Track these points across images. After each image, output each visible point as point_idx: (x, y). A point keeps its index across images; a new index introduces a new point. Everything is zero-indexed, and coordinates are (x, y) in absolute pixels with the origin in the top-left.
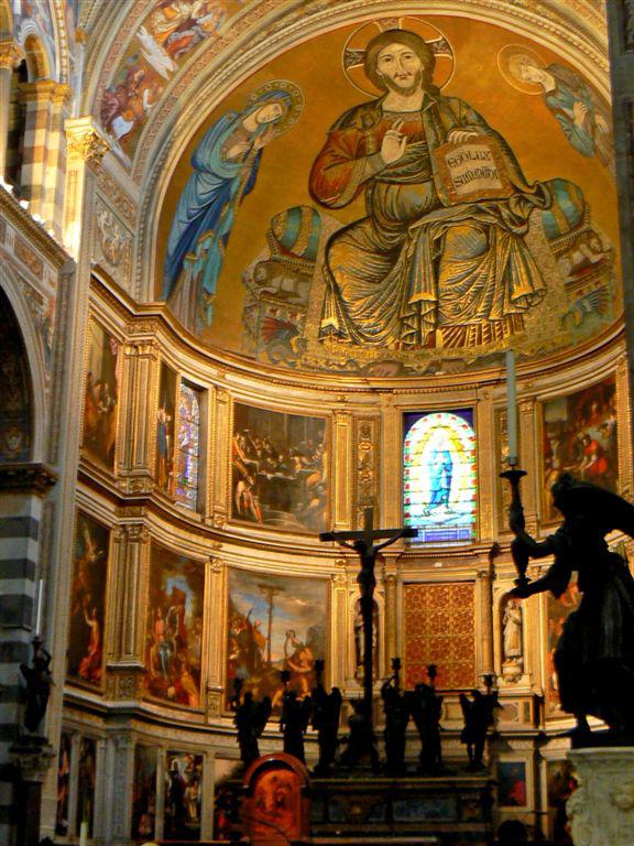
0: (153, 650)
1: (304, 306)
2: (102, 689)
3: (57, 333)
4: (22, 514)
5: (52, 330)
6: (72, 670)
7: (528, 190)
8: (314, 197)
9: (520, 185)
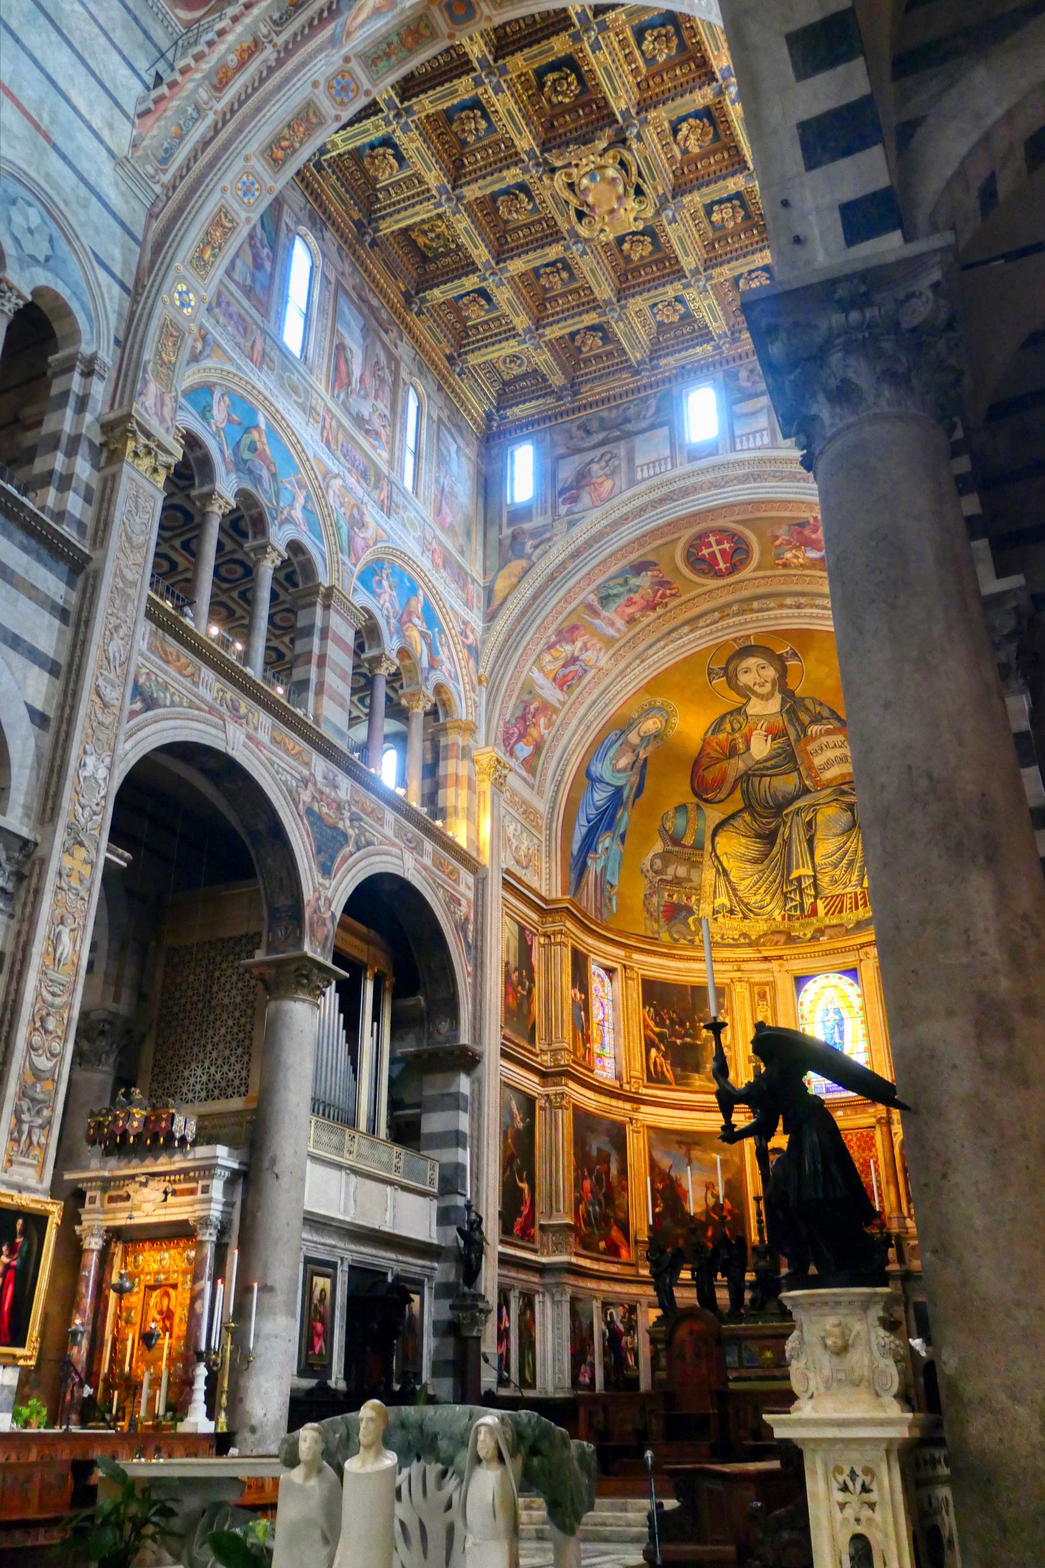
0: (581, 1207)
2: (537, 1246)
3: (476, 929)
4: (453, 1090)
5: (471, 927)
6: (506, 1229)
8: (696, 794)
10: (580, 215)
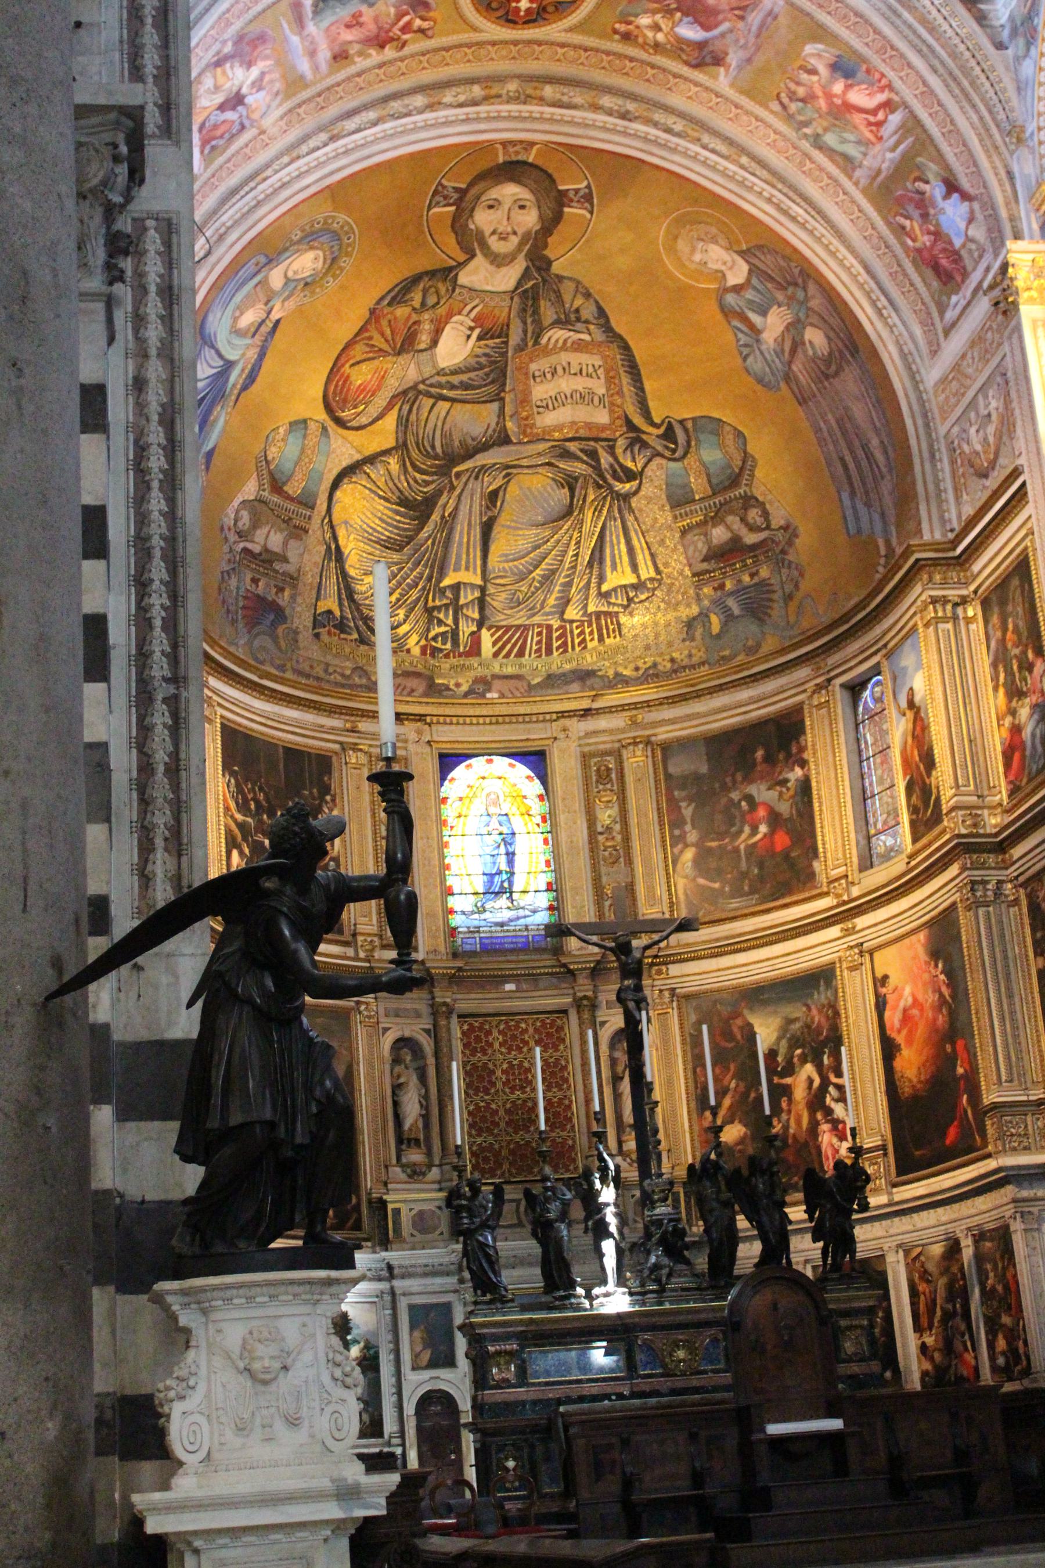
1: (292, 580)
7: (651, 430)
9: (638, 421)
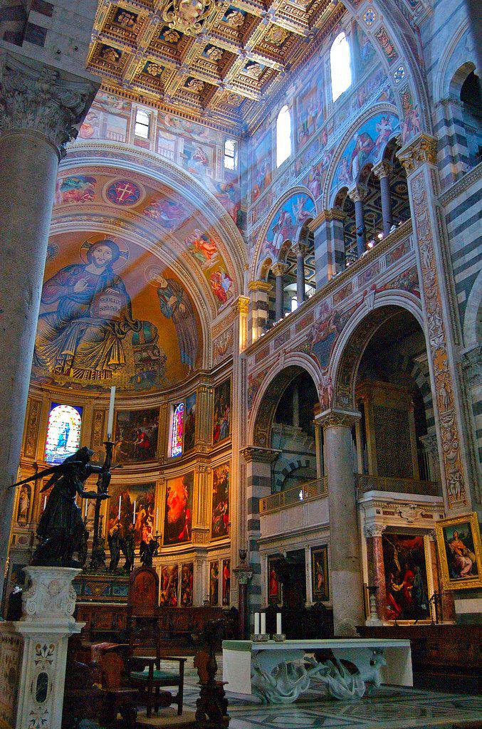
9: (128, 318)
10: (171, 9)
